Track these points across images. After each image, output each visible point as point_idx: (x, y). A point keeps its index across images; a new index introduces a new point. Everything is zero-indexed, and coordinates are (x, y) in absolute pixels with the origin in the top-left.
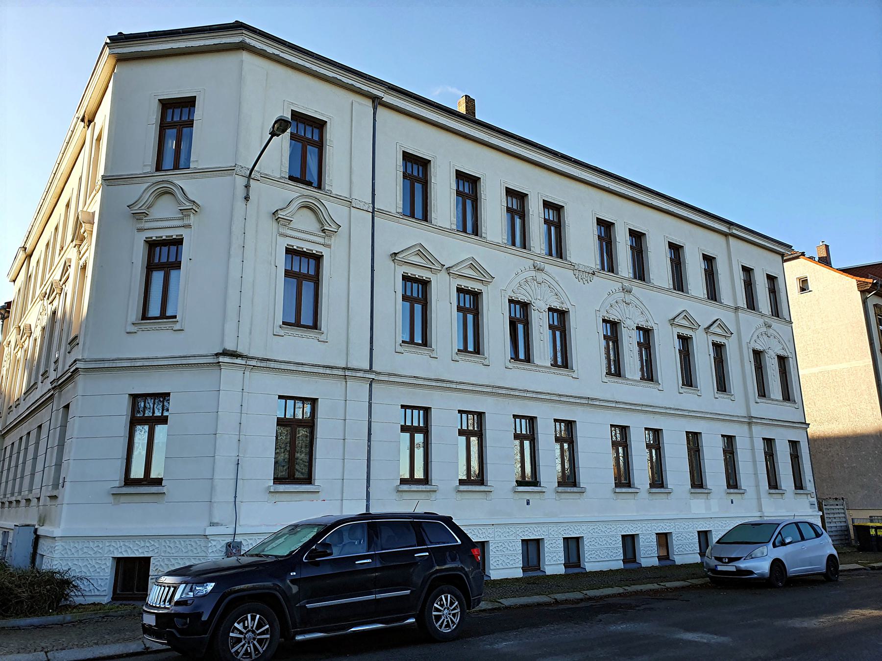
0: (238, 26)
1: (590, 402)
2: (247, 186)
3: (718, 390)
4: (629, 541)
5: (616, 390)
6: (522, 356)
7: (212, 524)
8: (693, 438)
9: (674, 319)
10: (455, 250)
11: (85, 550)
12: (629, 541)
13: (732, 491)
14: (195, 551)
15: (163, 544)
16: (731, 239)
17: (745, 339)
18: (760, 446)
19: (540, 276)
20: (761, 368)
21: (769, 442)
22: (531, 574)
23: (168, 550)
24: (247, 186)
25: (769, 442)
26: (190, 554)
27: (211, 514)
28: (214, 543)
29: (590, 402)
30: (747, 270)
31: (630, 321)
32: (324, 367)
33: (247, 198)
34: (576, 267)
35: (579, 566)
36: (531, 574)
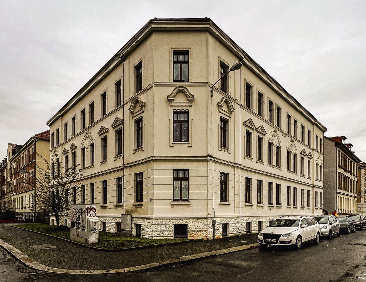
0: (207, 20)
1: (235, 166)
2: (212, 91)
3: (221, 146)
4: (249, 224)
5: (253, 164)
6: (292, 170)
7: (209, 214)
8: (260, 182)
9: (246, 122)
10: (258, 122)
11: (164, 222)
12: (249, 224)
13: (223, 203)
14: (158, 223)
15: (192, 220)
16: (315, 126)
17: (315, 160)
18: (243, 181)
19: (276, 134)
20: (249, 142)
21: (248, 180)
22: (225, 237)
23: (193, 222)
24: (212, 91)
25: (248, 180)
26: (201, 223)
27: (207, 211)
28: (209, 220)
29: (235, 166)
30: (317, 136)
31: (293, 151)
32: (229, 162)
33: (212, 96)
34: (283, 132)
35: (226, 235)
36: (225, 237)
